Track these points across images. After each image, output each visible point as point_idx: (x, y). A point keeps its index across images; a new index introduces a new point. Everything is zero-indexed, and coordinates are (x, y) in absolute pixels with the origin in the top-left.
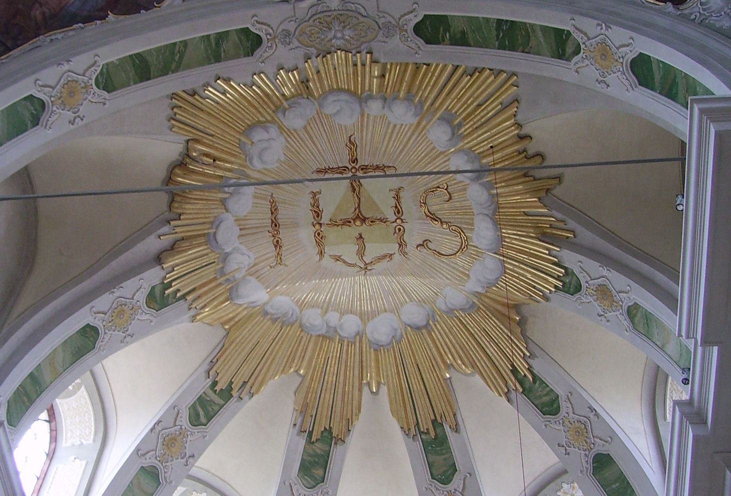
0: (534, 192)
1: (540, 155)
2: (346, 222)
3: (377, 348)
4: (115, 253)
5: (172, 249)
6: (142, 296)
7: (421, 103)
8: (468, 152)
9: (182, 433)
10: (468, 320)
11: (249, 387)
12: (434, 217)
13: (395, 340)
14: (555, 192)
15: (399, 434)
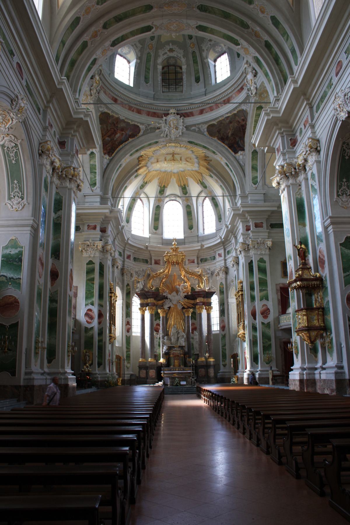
0: (206, 162)
1: (208, 157)
2: (171, 160)
3: (174, 173)
4: (129, 172)
5: (139, 169)
6: (134, 178)
7: (187, 148)
8: (195, 156)
9: (139, 191)
10: (192, 172)
11: (150, 181)
12: (187, 161)
13: (178, 173)
14: (211, 163)
15: (177, 186)
